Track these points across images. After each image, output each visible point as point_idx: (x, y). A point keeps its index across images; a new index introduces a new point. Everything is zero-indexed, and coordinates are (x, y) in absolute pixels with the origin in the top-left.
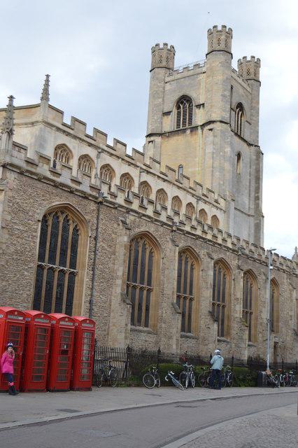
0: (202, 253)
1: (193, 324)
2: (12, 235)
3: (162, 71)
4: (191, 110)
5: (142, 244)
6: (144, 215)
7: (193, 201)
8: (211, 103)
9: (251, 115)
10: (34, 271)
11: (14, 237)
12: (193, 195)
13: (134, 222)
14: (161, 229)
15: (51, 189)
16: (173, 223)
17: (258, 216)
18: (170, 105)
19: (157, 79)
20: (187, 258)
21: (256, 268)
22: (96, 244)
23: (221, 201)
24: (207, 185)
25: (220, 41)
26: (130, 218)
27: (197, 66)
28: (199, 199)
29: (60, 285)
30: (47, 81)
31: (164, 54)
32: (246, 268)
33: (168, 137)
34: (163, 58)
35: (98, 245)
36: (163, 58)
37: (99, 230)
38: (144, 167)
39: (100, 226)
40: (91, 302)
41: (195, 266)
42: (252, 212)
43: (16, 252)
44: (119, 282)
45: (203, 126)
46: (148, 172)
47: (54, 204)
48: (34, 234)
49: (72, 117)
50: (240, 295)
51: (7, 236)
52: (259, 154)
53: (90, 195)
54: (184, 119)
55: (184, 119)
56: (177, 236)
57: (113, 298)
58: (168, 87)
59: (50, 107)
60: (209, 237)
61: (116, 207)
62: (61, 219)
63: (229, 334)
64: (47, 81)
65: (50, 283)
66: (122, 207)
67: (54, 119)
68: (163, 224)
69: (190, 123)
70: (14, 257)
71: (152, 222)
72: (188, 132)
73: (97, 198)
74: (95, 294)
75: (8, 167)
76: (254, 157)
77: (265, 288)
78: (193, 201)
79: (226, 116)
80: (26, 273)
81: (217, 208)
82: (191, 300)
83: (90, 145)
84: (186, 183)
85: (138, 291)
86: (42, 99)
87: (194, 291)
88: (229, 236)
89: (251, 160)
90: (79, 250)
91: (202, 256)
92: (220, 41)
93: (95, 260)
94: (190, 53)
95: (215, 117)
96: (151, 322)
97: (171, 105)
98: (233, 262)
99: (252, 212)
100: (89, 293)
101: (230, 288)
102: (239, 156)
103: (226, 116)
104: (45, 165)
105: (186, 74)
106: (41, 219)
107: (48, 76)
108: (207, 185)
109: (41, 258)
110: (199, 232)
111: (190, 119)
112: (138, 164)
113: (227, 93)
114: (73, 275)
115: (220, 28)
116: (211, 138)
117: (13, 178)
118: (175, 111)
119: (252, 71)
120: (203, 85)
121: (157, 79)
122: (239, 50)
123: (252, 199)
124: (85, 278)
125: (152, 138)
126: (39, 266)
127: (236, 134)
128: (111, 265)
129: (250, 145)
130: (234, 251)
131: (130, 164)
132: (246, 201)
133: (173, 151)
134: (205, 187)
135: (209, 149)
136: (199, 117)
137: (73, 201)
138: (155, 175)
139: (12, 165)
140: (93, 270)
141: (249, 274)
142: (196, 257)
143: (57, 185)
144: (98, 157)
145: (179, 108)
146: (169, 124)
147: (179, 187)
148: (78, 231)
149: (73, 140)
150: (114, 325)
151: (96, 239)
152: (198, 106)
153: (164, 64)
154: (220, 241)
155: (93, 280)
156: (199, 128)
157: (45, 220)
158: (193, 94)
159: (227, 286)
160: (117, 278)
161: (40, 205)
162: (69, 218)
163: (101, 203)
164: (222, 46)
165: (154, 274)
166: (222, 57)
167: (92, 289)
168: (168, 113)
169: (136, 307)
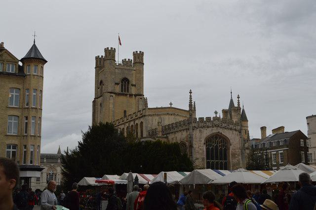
18: (118, 81)
25: (139, 57)
33: (118, 95)
45: (136, 95)
54: (125, 89)
55: (125, 89)
58: (117, 71)
92: (139, 57)
97: (119, 80)
120: (134, 75)
125: (112, 95)
145: (122, 82)
146: (118, 89)
152: (133, 85)
158: (130, 79)
168: (117, 84)
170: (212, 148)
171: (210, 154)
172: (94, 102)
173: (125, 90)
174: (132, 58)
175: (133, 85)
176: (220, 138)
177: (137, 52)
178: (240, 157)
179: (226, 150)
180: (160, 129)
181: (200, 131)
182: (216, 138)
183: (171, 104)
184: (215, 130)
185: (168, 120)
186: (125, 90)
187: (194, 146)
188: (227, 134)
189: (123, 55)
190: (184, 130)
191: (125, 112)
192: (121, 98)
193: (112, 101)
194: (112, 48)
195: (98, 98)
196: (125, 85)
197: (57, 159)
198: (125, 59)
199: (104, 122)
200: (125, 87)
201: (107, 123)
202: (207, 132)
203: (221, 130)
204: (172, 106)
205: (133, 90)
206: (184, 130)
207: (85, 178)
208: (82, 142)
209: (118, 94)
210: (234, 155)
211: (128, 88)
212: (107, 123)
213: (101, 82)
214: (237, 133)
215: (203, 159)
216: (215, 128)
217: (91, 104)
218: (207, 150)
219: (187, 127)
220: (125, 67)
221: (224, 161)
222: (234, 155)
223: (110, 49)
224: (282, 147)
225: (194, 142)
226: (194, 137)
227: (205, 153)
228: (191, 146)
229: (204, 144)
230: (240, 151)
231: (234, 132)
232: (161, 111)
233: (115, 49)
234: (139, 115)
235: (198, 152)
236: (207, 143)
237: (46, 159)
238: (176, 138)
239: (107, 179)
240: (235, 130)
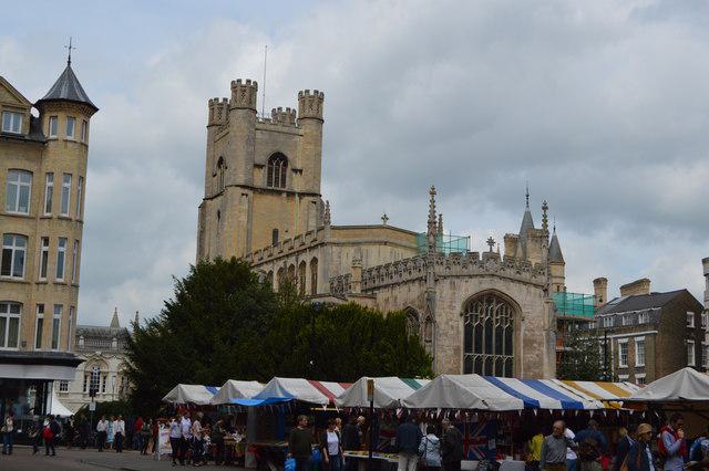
4: (284, 170)
18: (262, 158)
45: (302, 195)
54: (277, 178)
55: (277, 178)
69: (284, 184)
72: (284, 195)
92: (312, 102)
120: (300, 148)
125: (246, 191)
145: (270, 162)
146: (260, 178)
152: (295, 171)
158: (290, 157)
168: (260, 166)
170: (479, 326)
171: (473, 339)
172: (202, 207)
173: (277, 182)
174: (295, 105)
175: (295, 171)
176: (498, 303)
177: (307, 91)
178: (544, 349)
179: (510, 331)
180: (356, 276)
181: (453, 284)
182: (489, 302)
183: (385, 218)
184: (487, 284)
185: (377, 257)
186: (277, 182)
187: (438, 319)
188: (515, 292)
189: (275, 97)
190: (414, 281)
191: (275, 233)
192: (268, 200)
193: (245, 207)
194: (249, 81)
195: (212, 199)
197: (111, 340)
199: (227, 258)
200: (277, 174)
201: (233, 258)
202: (469, 288)
203: (500, 286)
204: (389, 223)
205: (296, 183)
206: (414, 281)
207: (182, 386)
208: (175, 300)
209: (263, 191)
210: (529, 343)
211: (284, 177)
212: (233, 258)
213: (221, 161)
214: (539, 291)
215: (457, 350)
216: (487, 279)
217: (196, 212)
218: (468, 328)
219: (423, 274)
220: (280, 128)
221: (505, 357)
222: (529, 343)
224: (643, 327)
225: (437, 310)
226: (438, 297)
227: (462, 336)
228: (430, 320)
229: (461, 315)
230: (544, 333)
231: (532, 289)
232: (360, 235)
233: (255, 83)
234: (308, 241)
235: (446, 334)
236: (466, 311)
237: (85, 337)
238: (396, 298)
239: (236, 393)
240: (536, 286)
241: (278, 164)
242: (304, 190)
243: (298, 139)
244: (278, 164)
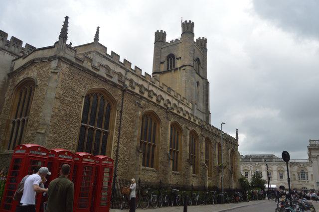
0: (183, 126)
1: (179, 167)
2: (63, 104)
3: (160, 43)
5: (150, 120)
6: (151, 101)
7: (176, 102)
8: (184, 57)
9: (203, 64)
10: (78, 129)
11: (64, 105)
12: (176, 100)
13: (145, 105)
14: (161, 110)
15: (92, 78)
16: (168, 108)
17: (207, 113)
18: (164, 59)
19: (158, 46)
20: (175, 129)
21: (211, 137)
22: (121, 115)
23: (191, 105)
24: (183, 95)
25: (188, 28)
26: (143, 102)
27: (177, 40)
28: (179, 102)
29: (98, 140)
30: (98, 30)
31: (161, 35)
32: (206, 136)
34: (160, 37)
35: (123, 116)
36: (160, 37)
37: (124, 107)
38: (151, 83)
39: (124, 104)
40: (117, 151)
41: (180, 134)
42: (205, 112)
43: (66, 115)
44: (136, 139)
45: (180, 68)
46: (153, 85)
47: (94, 87)
48: (80, 105)
49: (112, 52)
50: (204, 151)
51: (59, 104)
52: (207, 83)
53: (118, 85)
55: (171, 65)
56: (170, 115)
57: (131, 149)
58: (163, 50)
59: (99, 44)
60: (187, 117)
61: (134, 94)
62: (100, 98)
63: (197, 172)
64: (98, 30)
65: (90, 138)
66: (138, 95)
67: (101, 51)
68: (162, 108)
69: (174, 67)
70: (64, 118)
71: (155, 105)
73: (122, 88)
74: (120, 146)
75: (62, 59)
76: (205, 85)
77: (216, 147)
78: (176, 102)
79: (192, 63)
80: (72, 129)
81: (188, 107)
82: (178, 152)
83: (121, 67)
84: (172, 94)
85: (147, 146)
86: (95, 39)
87: (179, 147)
88: (197, 118)
89: (203, 85)
90: (111, 118)
91: (183, 128)
92: (188, 28)
93: (120, 124)
94: (174, 34)
95: (186, 63)
96: (155, 165)
98: (199, 133)
99: (205, 112)
100: (116, 145)
101: (198, 147)
102: (198, 83)
103: (192, 63)
104: (88, 63)
105: (172, 44)
106: (85, 96)
107: (98, 28)
108: (183, 95)
109: (84, 120)
110: (181, 115)
111: (174, 65)
112: (148, 81)
113: (192, 52)
114: (107, 133)
115: (188, 22)
116: (185, 73)
117: (65, 67)
118: (166, 61)
119: (203, 44)
120: (180, 48)
121: (158, 46)
122: (198, 34)
123: (205, 104)
124: (114, 134)
125: (155, 75)
126: (83, 128)
127: (196, 73)
128: (131, 129)
129: (203, 79)
130: (199, 127)
131: (143, 80)
132: (201, 105)
133: (166, 79)
134: (182, 97)
135: (184, 79)
136: (178, 64)
137: (107, 87)
138: (156, 87)
139: (64, 58)
140: (119, 131)
141: (208, 141)
142: (180, 129)
143: (96, 76)
144: (126, 74)
145: (168, 60)
146: (163, 68)
147: (169, 95)
148: (110, 107)
149: (112, 63)
150: (132, 166)
151: (121, 112)
152: (178, 59)
153: (161, 39)
154: (192, 120)
155: (119, 137)
156: (179, 70)
157: (88, 97)
158: (175, 53)
159: (196, 146)
160: (134, 136)
161: (85, 87)
162: (104, 98)
163: (125, 90)
164: (189, 30)
165: (157, 136)
166: (190, 35)
167: (118, 143)
168: (163, 63)
169: (146, 155)
173: (171, 67)
186: (171, 67)
196: (171, 62)
198: (200, 38)
223: (160, 32)
233: (165, 32)
241: (171, 59)
242: (181, 66)
243: (179, 45)
244: (171, 59)
